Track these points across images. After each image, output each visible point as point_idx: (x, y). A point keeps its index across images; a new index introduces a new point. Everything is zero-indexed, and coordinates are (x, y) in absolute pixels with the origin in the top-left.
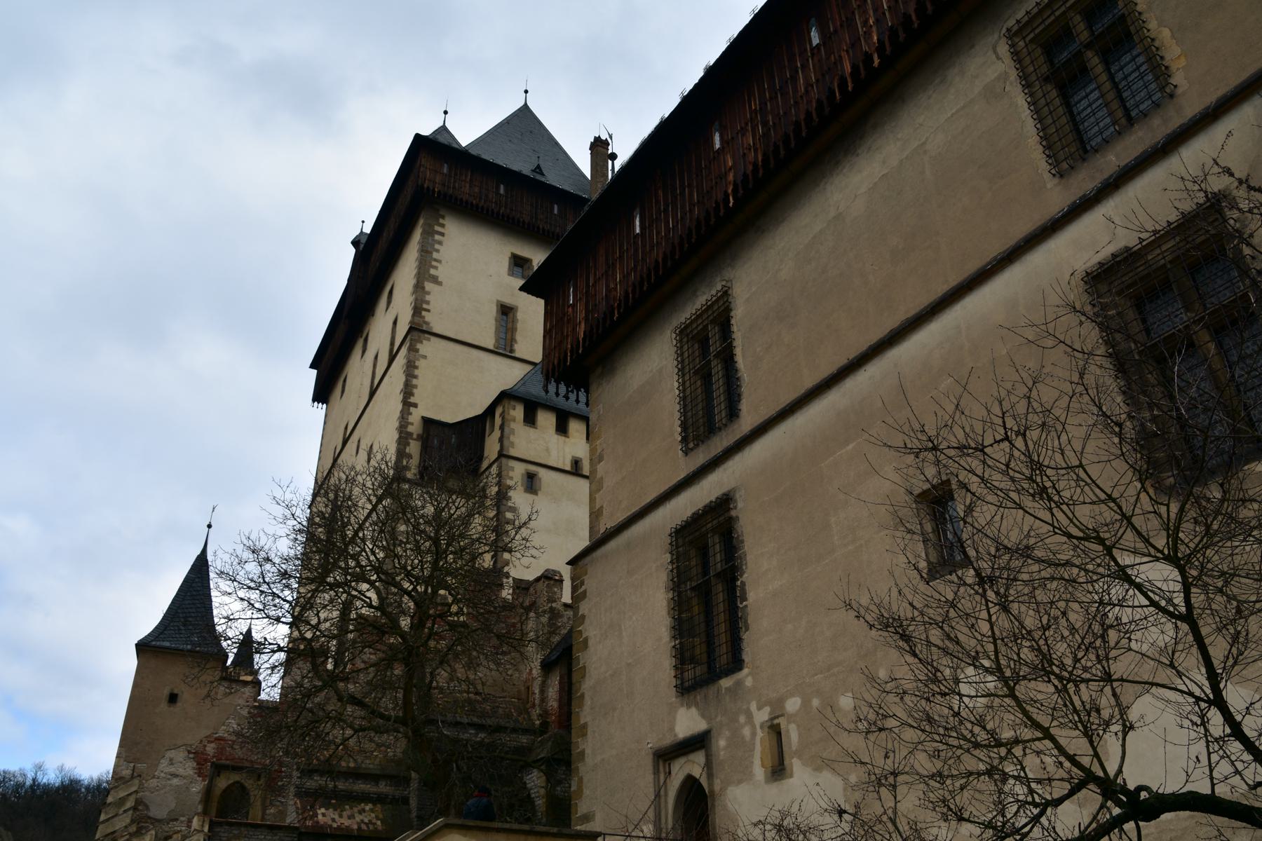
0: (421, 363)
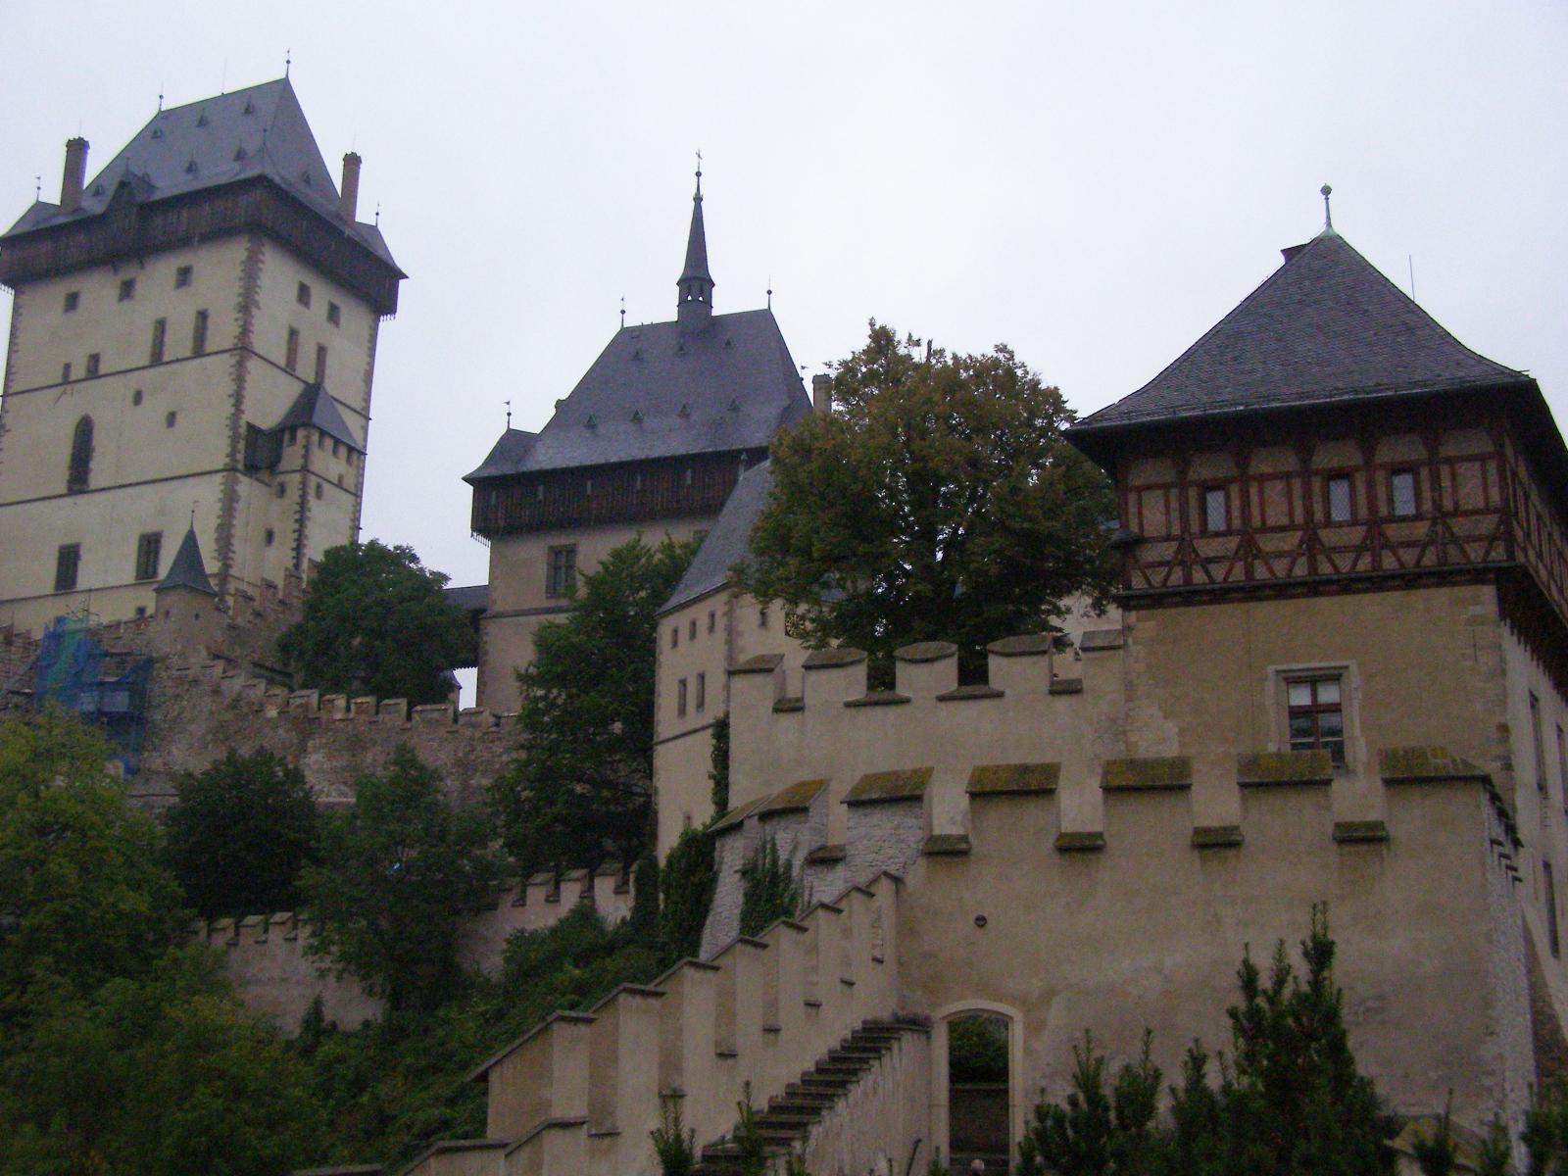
0: (248, 378)
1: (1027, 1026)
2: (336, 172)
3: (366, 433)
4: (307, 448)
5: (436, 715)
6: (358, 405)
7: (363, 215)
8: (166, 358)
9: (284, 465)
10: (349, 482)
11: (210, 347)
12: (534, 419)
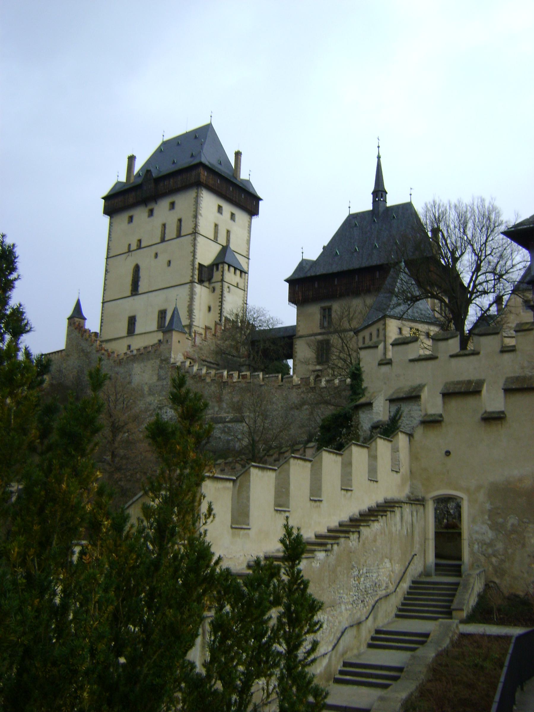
1: (469, 501)
2: (232, 159)
3: (248, 265)
4: (223, 272)
5: (273, 378)
6: (245, 254)
7: (244, 175)
8: (166, 239)
9: (214, 280)
10: (241, 285)
11: (182, 234)
12: (313, 254)
